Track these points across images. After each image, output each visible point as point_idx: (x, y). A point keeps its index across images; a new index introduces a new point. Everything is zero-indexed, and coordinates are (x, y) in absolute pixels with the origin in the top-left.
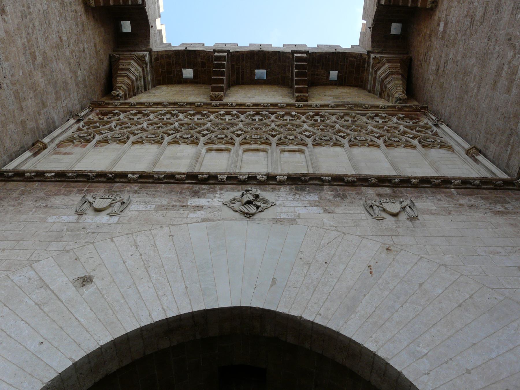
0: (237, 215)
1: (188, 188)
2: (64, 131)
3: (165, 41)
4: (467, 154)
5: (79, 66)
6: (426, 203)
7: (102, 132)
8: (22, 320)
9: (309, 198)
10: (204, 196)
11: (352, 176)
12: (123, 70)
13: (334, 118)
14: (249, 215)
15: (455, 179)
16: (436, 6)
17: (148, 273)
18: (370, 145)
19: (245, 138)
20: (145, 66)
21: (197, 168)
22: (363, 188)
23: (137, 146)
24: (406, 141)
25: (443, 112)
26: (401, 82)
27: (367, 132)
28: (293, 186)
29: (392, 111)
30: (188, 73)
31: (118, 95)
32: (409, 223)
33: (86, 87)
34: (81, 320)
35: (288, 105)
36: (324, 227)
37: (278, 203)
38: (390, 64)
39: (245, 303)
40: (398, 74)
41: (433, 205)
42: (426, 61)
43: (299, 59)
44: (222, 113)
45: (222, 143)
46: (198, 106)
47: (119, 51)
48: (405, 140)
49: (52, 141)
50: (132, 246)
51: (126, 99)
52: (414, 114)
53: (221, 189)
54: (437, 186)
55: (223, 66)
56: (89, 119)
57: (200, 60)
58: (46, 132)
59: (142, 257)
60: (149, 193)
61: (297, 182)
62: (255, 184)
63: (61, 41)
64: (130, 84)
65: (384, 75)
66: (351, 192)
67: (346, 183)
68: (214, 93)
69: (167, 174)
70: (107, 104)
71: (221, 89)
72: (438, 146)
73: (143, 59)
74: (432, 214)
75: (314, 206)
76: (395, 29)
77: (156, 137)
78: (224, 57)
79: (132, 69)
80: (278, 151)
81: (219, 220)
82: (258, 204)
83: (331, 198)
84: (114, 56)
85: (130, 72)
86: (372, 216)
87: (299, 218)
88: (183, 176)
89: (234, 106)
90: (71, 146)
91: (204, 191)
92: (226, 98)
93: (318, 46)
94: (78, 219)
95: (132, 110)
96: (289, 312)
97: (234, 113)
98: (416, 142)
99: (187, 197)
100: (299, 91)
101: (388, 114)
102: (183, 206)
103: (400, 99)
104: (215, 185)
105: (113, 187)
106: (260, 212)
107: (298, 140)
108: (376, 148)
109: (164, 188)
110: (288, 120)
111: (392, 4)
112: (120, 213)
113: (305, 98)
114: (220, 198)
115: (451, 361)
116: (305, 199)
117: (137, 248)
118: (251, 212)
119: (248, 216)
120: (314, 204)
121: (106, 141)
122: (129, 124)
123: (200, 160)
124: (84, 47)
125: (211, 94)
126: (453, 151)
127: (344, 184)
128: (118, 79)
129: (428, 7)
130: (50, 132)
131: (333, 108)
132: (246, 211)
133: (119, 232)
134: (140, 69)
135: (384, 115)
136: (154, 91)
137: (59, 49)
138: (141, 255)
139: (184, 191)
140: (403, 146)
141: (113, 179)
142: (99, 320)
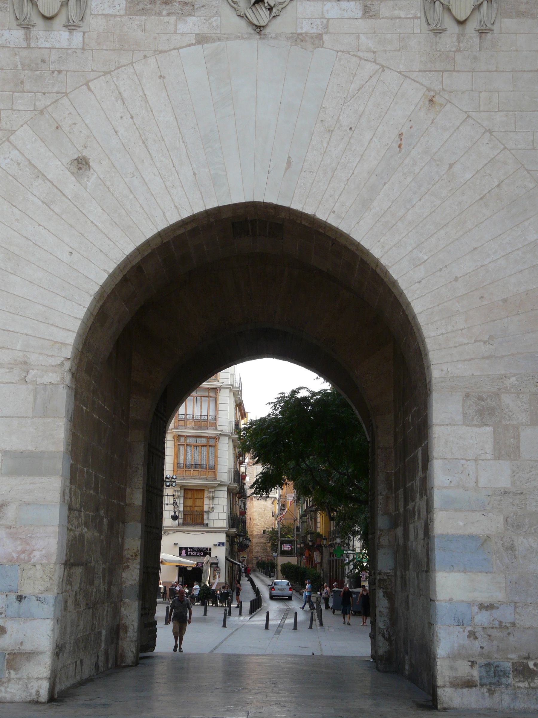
0: (242, 23)
8: (39, 225)
14: (259, 29)
17: (149, 151)
32: (476, 35)
34: (97, 224)
39: (259, 199)
50: (117, 100)
59: (135, 120)
81: (219, 39)
87: (327, 33)
94: (27, 39)
96: (303, 209)
112: (81, 24)
115: (445, 269)
117: (124, 103)
118: (262, 24)
119: (258, 30)
133: (93, 71)
138: (132, 117)
142: (116, 223)
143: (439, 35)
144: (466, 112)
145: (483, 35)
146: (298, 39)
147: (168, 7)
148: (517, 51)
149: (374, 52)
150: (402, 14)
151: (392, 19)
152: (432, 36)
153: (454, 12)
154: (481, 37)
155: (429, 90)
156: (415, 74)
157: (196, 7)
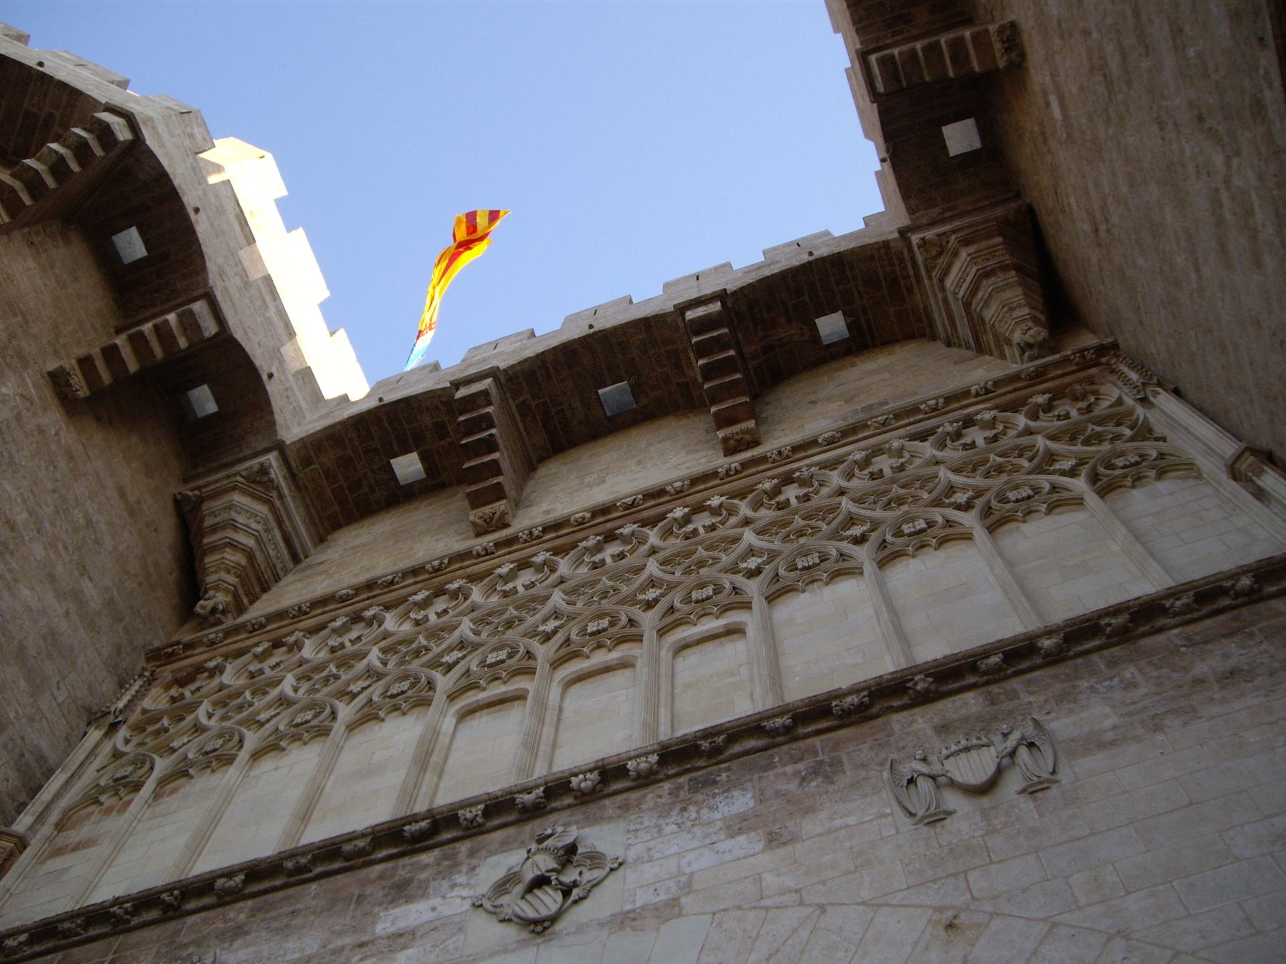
1: (381, 877)
2: (72, 776)
3: (329, 392)
4: (1235, 479)
5: (83, 570)
6: (1086, 710)
7: (175, 744)
9: (726, 809)
10: (423, 891)
11: (854, 690)
12: (214, 529)
13: (835, 478)
15: (1173, 593)
16: (1023, 56)
18: (943, 542)
19: (567, 641)
20: (274, 494)
21: (425, 788)
22: (895, 717)
23: (267, 764)
24: (1054, 488)
25: (1154, 351)
26: (1019, 291)
27: (934, 494)
28: (682, 780)
29: (1009, 396)
30: (408, 466)
31: (214, 610)
33: (119, 619)
35: (695, 481)
36: (762, 903)
37: (631, 855)
38: (972, 249)
40: (1004, 269)
41: (1108, 710)
42: (1063, 211)
43: (703, 325)
44: (504, 570)
45: (494, 682)
46: (437, 570)
47: (196, 477)
48: (1047, 487)
49: (41, 818)
51: (241, 609)
52: (1080, 381)
53: (472, 853)
54: (1124, 636)
55: (488, 422)
56: (144, 711)
57: (427, 420)
58: (23, 798)
60: (275, 924)
61: (689, 761)
62: (569, 806)
63: (13, 528)
64: (244, 562)
65: (965, 285)
66: (856, 746)
67: (840, 717)
68: (479, 512)
69: (319, 848)
70: (189, 646)
71: (498, 493)
72: (1153, 473)
73: (265, 479)
74: (1102, 746)
75: (741, 831)
76: (960, 137)
77: (315, 716)
78: (485, 393)
79: (241, 519)
80: (665, 654)
82: (569, 876)
83: (792, 786)
84: (188, 498)
85: (236, 529)
86: (912, 815)
88: (361, 843)
89: (538, 537)
90: (93, 819)
91: (423, 876)
92: (521, 513)
93: (765, 253)
95: (257, 645)
97: (539, 559)
98: (1079, 484)
99: (376, 910)
100: (723, 420)
101: (1003, 408)
102: (362, 945)
103: (1030, 346)
104: (457, 845)
105: (180, 931)
106: (575, 902)
107: (722, 598)
108: (962, 545)
109: (314, 898)
110: (701, 530)
111: (905, 84)
113: (748, 437)
114: (468, 885)
116: (717, 815)
118: (544, 913)
119: (539, 928)
120: (737, 826)
121: (182, 772)
122: (248, 695)
123: (435, 758)
124: (86, 513)
125: (471, 518)
126: (1199, 476)
127: (835, 723)
128: (207, 560)
129: (1002, 63)
130: (34, 791)
131: (831, 442)
132: (531, 914)
134: (263, 509)
135: (988, 416)
136: (323, 557)
137: (12, 553)
139: (368, 891)
140: (1043, 507)
141: (179, 907)
143: (938, 825)
144: (1045, 920)
145: (1039, 795)
146: (626, 920)
147: (364, 949)
148: (1126, 792)
149: (797, 891)
150: (851, 820)
151: (830, 832)
152: (926, 829)
153: (958, 778)
154: (1035, 799)
155: (940, 910)
156: (901, 894)
157: (419, 934)
